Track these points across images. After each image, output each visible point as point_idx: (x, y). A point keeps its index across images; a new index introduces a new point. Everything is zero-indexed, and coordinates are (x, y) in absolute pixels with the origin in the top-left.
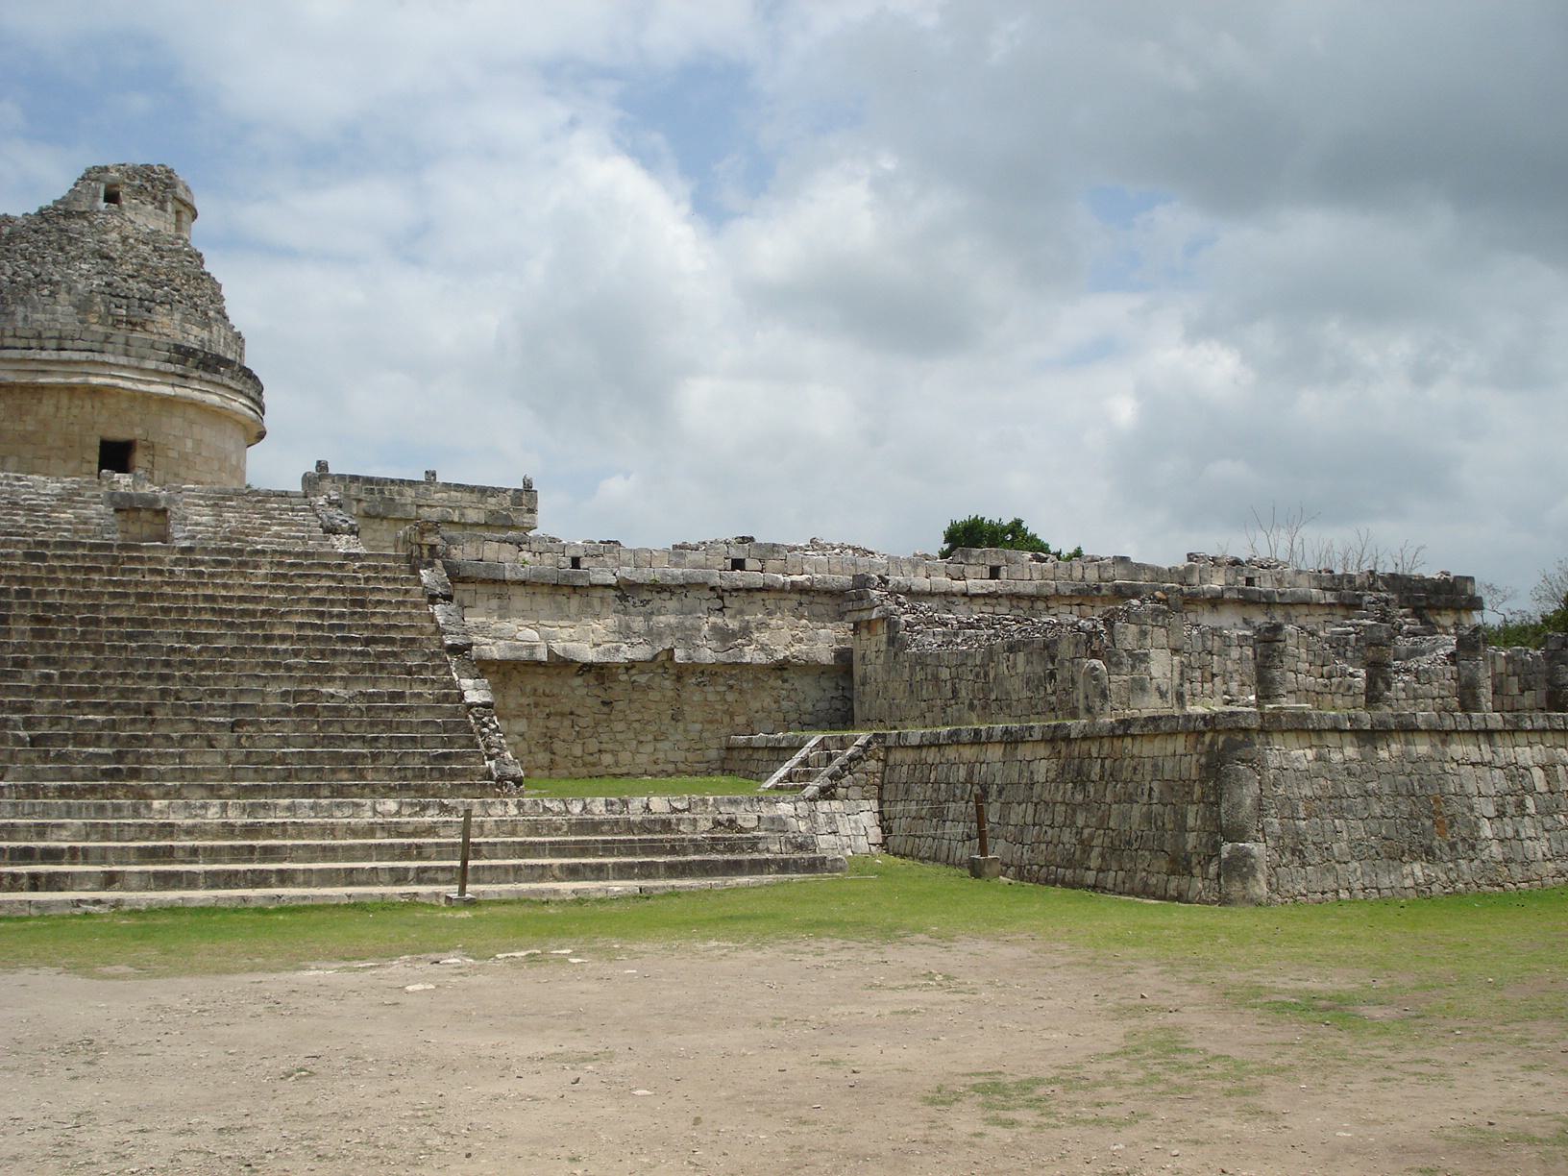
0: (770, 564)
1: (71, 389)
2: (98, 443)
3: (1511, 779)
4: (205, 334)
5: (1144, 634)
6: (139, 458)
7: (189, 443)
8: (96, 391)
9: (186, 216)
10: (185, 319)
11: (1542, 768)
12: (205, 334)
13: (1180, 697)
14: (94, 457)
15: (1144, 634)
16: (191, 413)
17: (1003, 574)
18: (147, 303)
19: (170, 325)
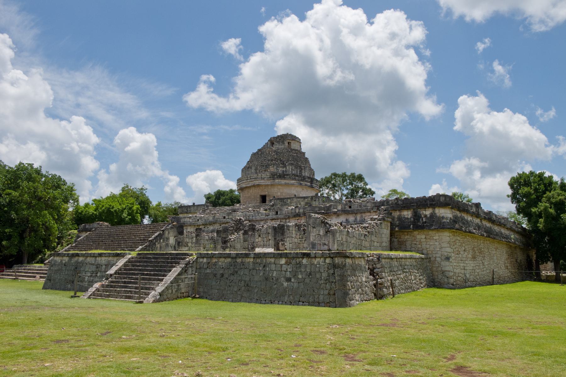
0: (230, 217)
1: (254, 186)
2: (259, 196)
3: (97, 268)
4: (284, 169)
5: (169, 233)
6: (267, 199)
7: (279, 194)
8: (258, 185)
9: (292, 142)
10: (277, 167)
11: (106, 265)
12: (284, 169)
13: (175, 247)
14: (259, 199)
15: (169, 233)
16: (280, 187)
17: (279, 213)
18: (267, 166)
19: (272, 169)
